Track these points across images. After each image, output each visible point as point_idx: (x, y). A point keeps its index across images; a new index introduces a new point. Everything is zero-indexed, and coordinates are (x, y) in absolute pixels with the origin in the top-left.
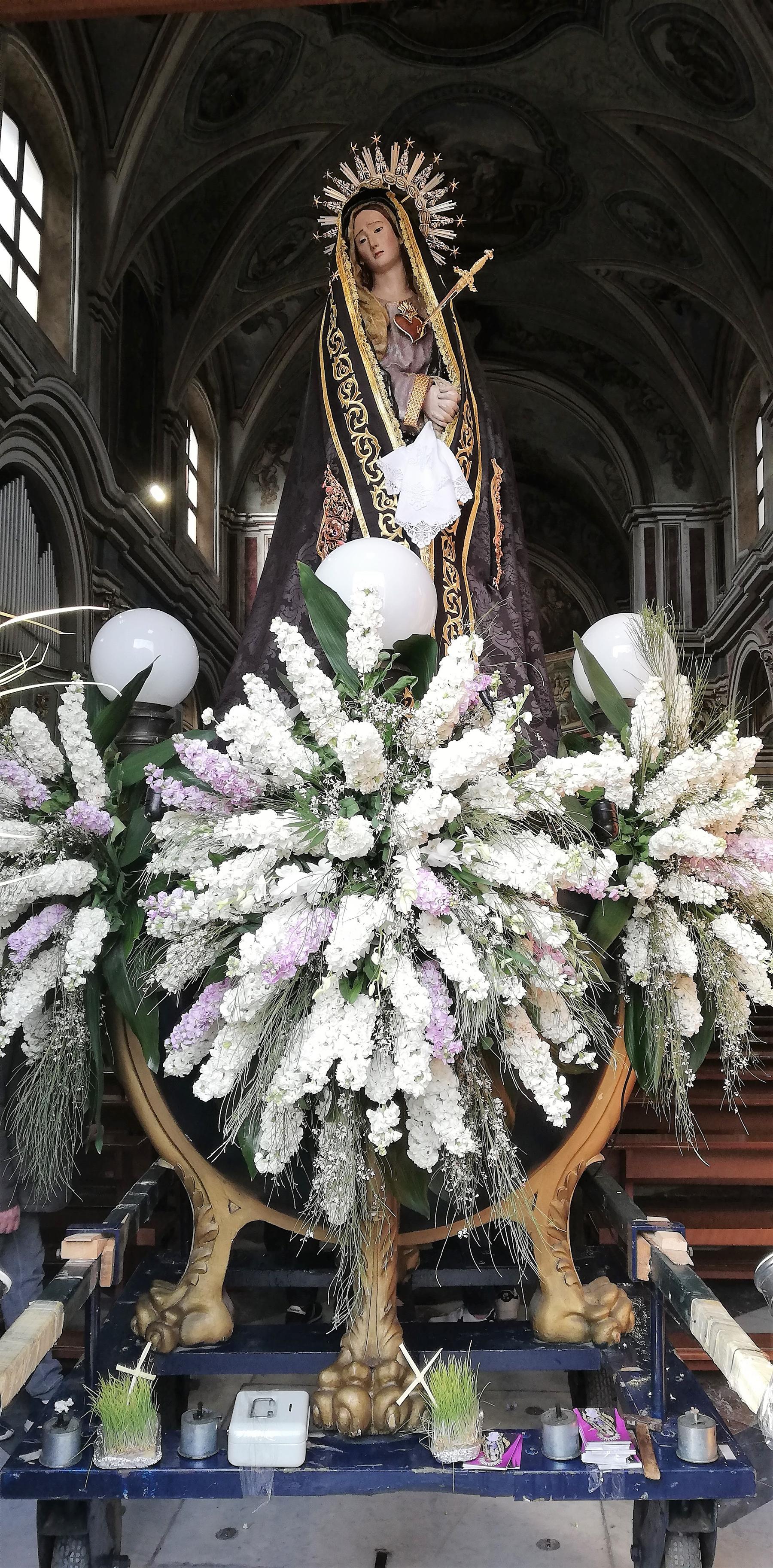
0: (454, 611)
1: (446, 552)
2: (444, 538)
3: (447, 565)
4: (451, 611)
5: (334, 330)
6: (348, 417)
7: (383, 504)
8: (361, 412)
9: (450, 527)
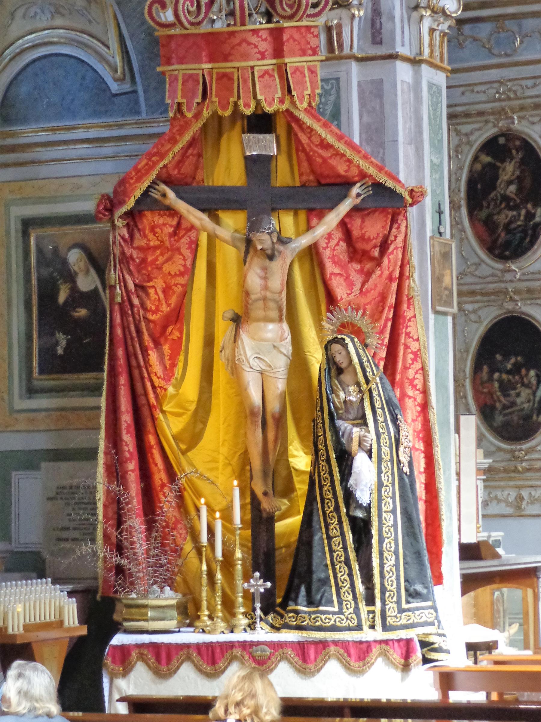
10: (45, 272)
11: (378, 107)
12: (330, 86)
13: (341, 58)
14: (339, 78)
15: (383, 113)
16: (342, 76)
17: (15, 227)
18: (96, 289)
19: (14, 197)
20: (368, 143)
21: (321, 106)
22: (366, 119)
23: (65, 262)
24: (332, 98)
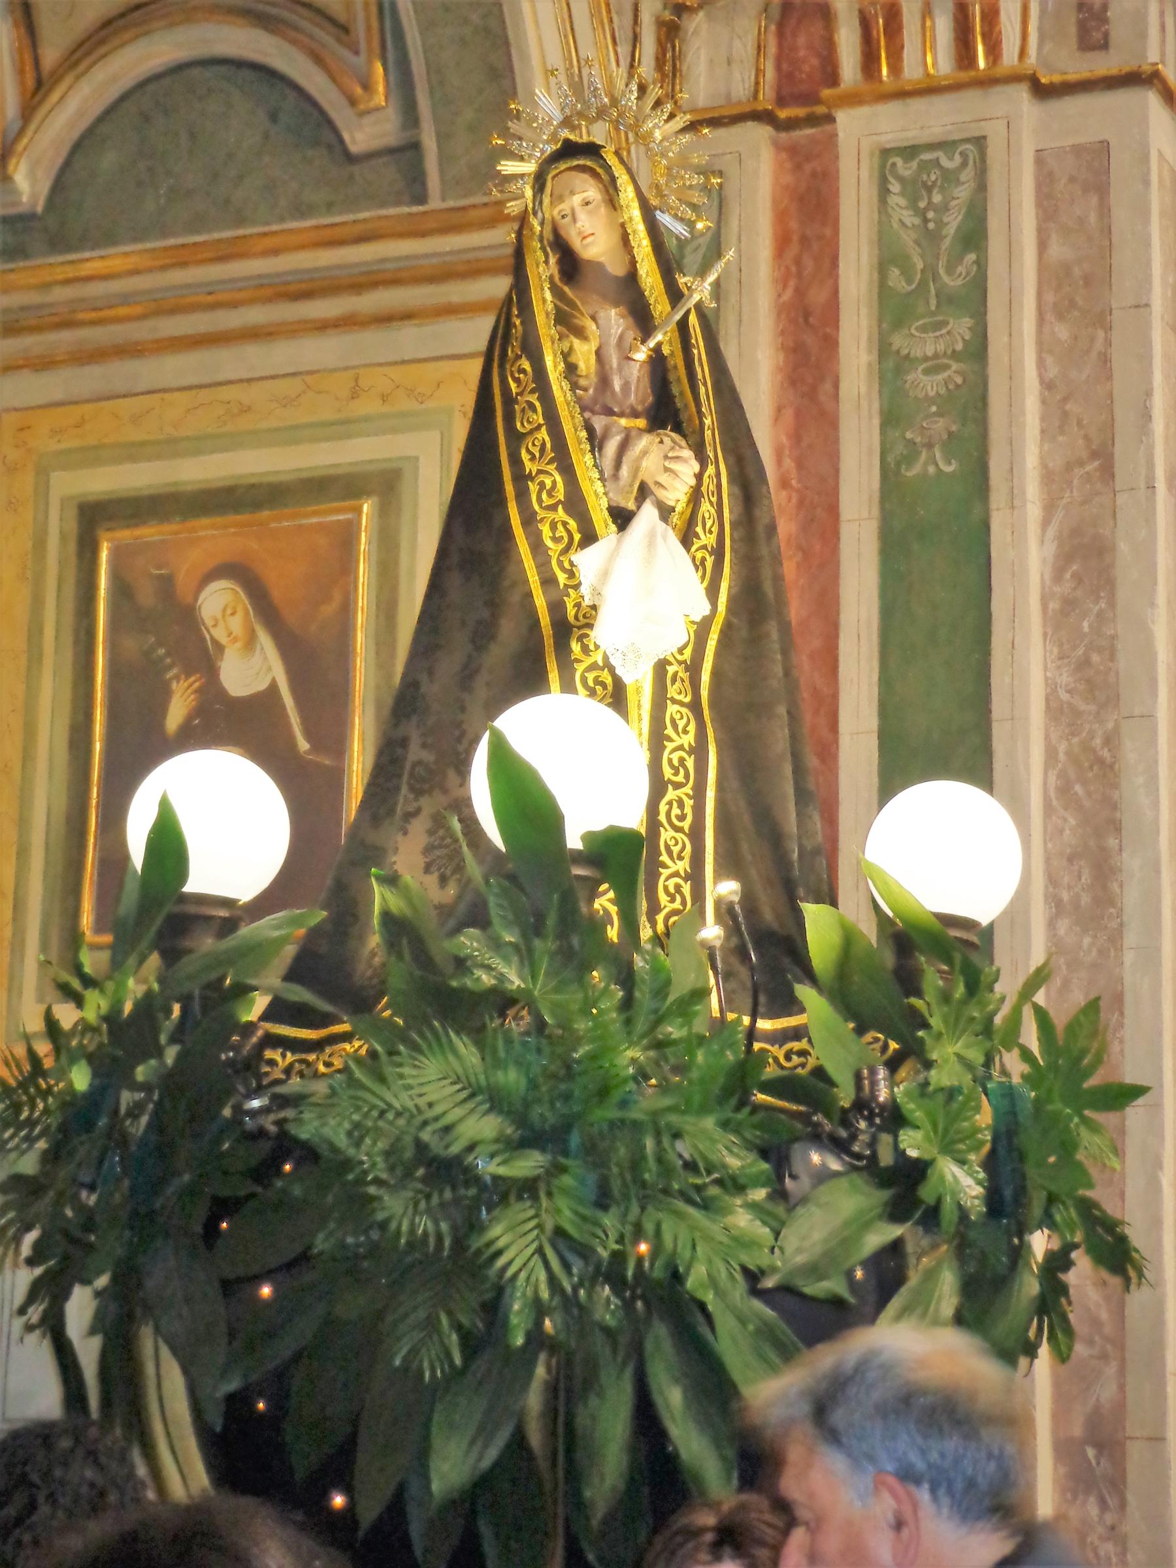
0: (680, 778)
1: (672, 691)
2: (671, 670)
3: (672, 709)
5: (518, 357)
6: (533, 488)
7: (581, 618)
8: (554, 483)
9: (681, 651)
10: (131, 644)
11: (1093, 218)
12: (958, 159)
13: (988, 82)
14: (984, 137)
16: (996, 134)
17: (59, 526)
18: (273, 688)
19: (64, 446)
20: (1060, 317)
21: (931, 215)
22: (1057, 250)
23: (189, 617)
24: (963, 192)
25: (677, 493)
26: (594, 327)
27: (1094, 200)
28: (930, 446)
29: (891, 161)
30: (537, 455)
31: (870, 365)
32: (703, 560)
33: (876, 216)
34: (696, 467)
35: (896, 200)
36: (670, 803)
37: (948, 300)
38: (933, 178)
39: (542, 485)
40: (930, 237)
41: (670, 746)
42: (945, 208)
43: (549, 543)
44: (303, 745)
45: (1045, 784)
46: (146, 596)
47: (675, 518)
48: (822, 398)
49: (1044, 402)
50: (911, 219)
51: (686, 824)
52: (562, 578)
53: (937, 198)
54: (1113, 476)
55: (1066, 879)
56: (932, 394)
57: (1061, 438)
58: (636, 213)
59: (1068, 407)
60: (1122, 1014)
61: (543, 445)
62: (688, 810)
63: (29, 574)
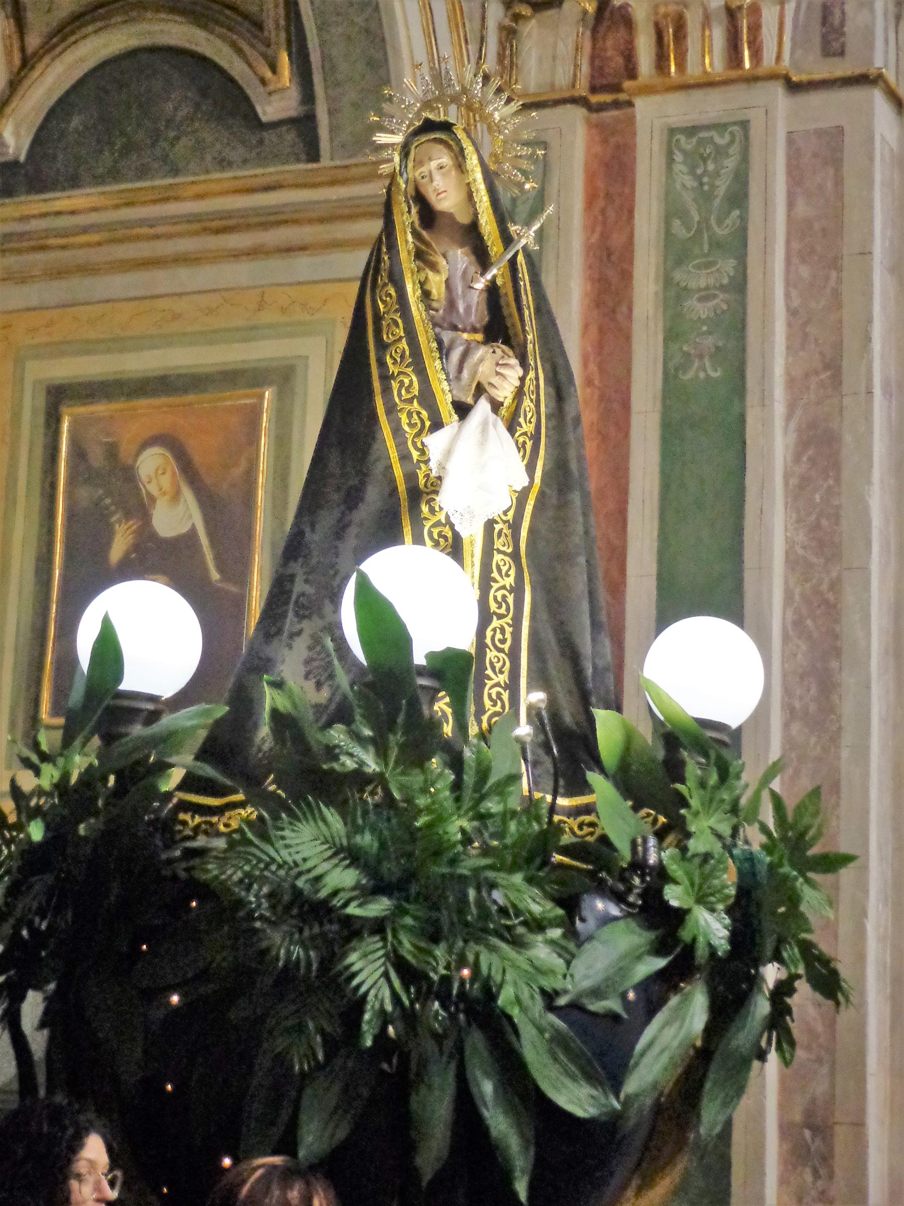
0: (503, 611)
1: (498, 544)
2: (497, 527)
3: (497, 557)
4: (498, 611)
5: (385, 285)
6: (395, 385)
8: (411, 382)
9: (505, 513)
11: (830, 184)
12: (727, 137)
13: (753, 79)
14: (748, 121)
15: (840, 196)
16: (757, 118)
17: (32, 404)
18: (193, 533)
19: (36, 341)
20: (803, 261)
21: (705, 179)
22: (802, 209)
23: (129, 475)
24: (730, 163)
25: (505, 392)
26: (445, 263)
27: (831, 171)
28: (701, 357)
29: (678, 137)
30: (399, 360)
31: (656, 293)
32: (524, 443)
33: (664, 179)
34: (520, 372)
35: (680, 167)
36: (494, 630)
37: (717, 245)
38: (708, 151)
39: (402, 383)
40: (705, 197)
41: (495, 586)
42: (717, 174)
43: (406, 428)
44: (215, 575)
45: (784, 618)
46: (97, 457)
47: (503, 411)
48: (619, 317)
49: (789, 325)
50: (690, 182)
51: (506, 647)
52: (415, 455)
53: (711, 167)
54: (841, 383)
55: (798, 692)
56: (703, 316)
57: (801, 353)
58: (479, 176)
59: (808, 330)
60: (839, 797)
61: (404, 351)
62: (508, 635)
63: (7, 439)
